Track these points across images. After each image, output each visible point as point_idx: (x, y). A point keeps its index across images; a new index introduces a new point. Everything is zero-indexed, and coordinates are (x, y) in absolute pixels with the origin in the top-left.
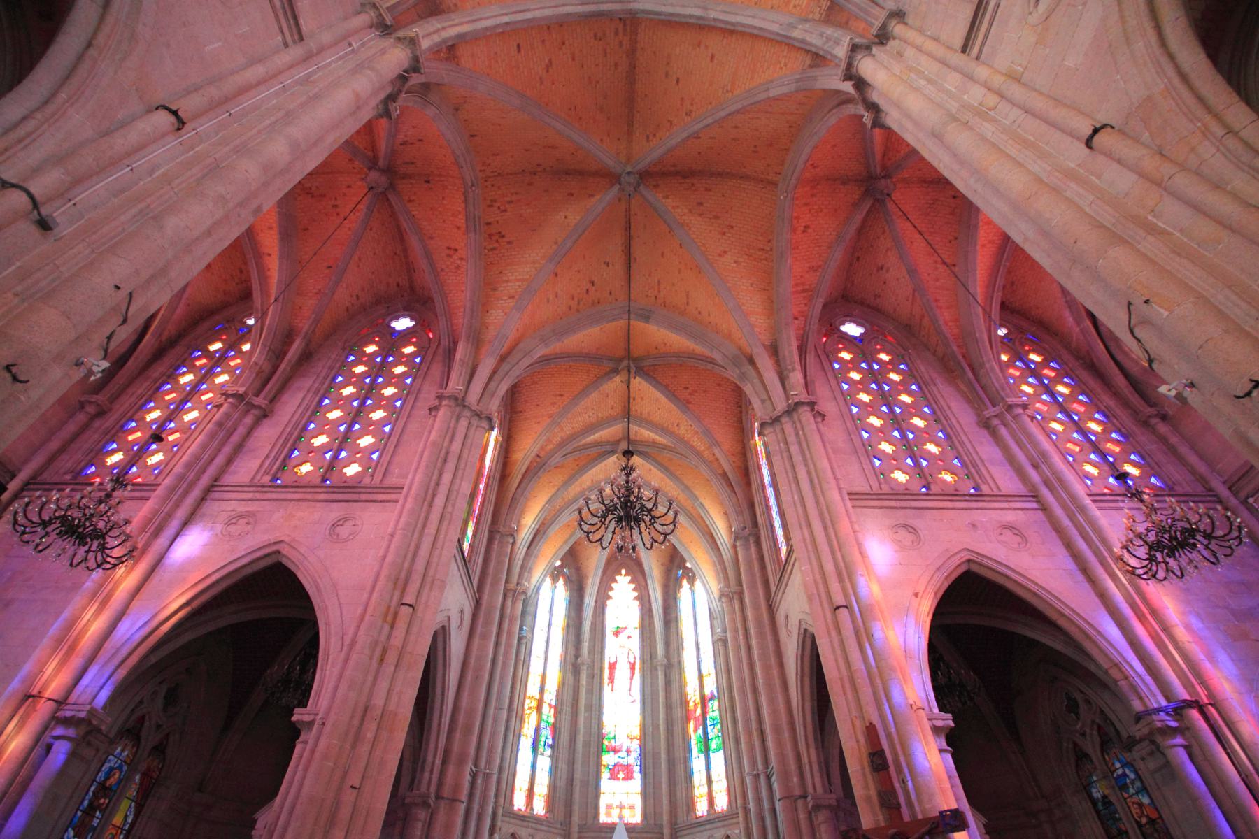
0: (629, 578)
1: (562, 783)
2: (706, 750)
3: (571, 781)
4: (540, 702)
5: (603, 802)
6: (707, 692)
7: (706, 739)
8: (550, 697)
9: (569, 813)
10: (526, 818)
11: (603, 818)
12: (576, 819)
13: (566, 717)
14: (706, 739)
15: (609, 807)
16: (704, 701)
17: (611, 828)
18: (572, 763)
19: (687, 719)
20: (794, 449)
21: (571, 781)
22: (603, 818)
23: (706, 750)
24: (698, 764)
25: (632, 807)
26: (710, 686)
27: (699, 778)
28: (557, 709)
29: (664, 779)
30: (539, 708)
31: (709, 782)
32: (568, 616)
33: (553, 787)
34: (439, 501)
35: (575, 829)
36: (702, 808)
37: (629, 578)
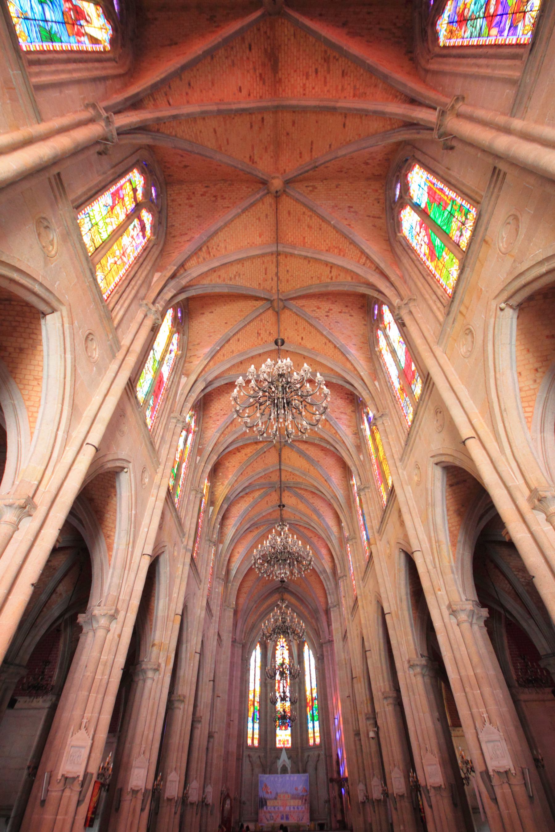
0: (284, 640)
1: (263, 733)
2: (313, 720)
3: (266, 732)
4: (254, 701)
5: (278, 739)
6: (314, 696)
7: (313, 716)
8: (257, 699)
9: (266, 744)
10: (252, 748)
11: (278, 745)
12: (268, 746)
13: (263, 706)
14: (313, 716)
15: (280, 741)
16: (312, 700)
17: (281, 749)
18: (266, 724)
19: (306, 707)
20: (330, 657)
21: (266, 732)
22: (278, 745)
23: (313, 720)
24: (310, 725)
25: (288, 741)
26: (315, 695)
27: (310, 731)
28: (259, 703)
29: (299, 731)
30: (254, 704)
31: (314, 733)
32: (262, 661)
33: (260, 735)
34: (234, 683)
35: (268, 750)
36: (311, 742)
37: (284, 640)
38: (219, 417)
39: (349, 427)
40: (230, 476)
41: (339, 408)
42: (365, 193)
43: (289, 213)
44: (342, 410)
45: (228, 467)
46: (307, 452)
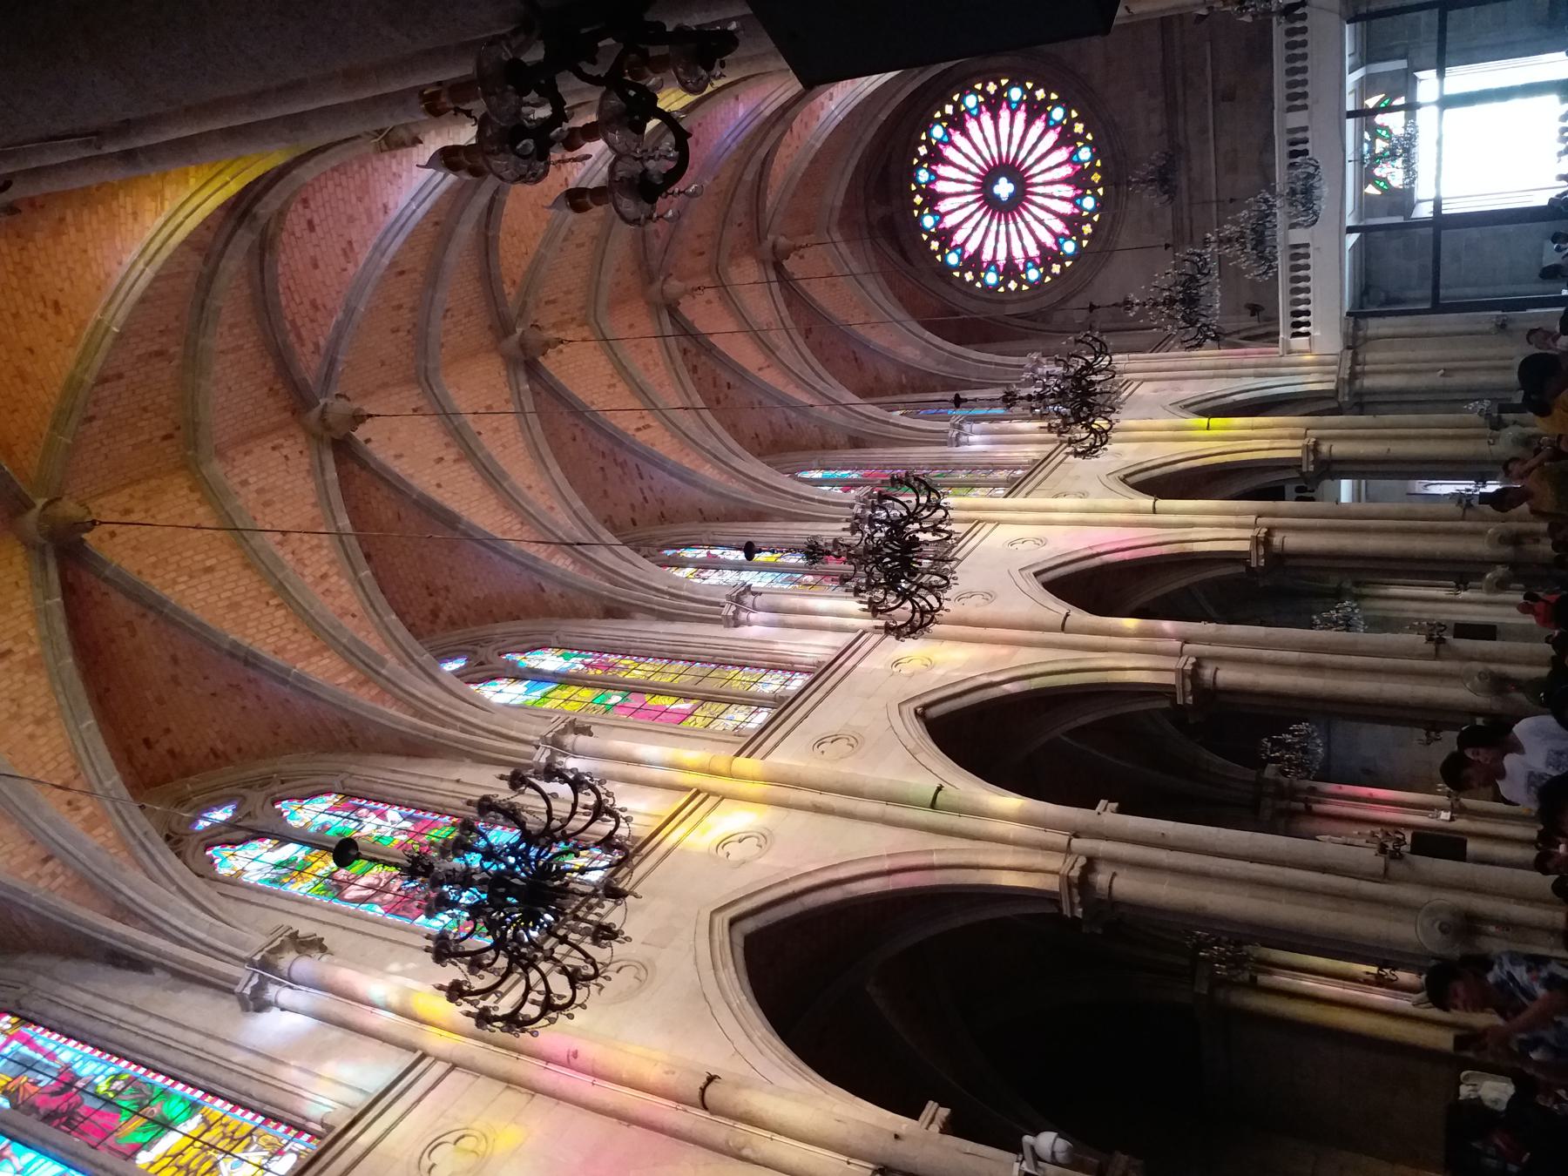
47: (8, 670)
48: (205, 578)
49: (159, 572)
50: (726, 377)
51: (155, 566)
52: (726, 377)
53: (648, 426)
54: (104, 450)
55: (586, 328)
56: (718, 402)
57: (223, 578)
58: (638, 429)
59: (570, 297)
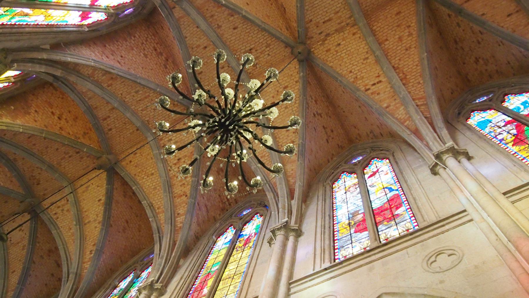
38: (112, 57)
39: (199, 225)
40: (18, 122)
41: (208, 200)
42: (450, 77)
43: (398, 13)
44: (209, 204)
45: (29, 114)
46: (114, 205)
47: (99, 205)
48: (151, 177)
49: (140, 175)
50: (477, 28)
51: (139, 172)
52: (477, 28)
53: (380, 82)
54: (122, 136)
55: (356, 27)
56: (479, 43)
57: (155, 178)
58: (374, 84)
59: (340, 14)
